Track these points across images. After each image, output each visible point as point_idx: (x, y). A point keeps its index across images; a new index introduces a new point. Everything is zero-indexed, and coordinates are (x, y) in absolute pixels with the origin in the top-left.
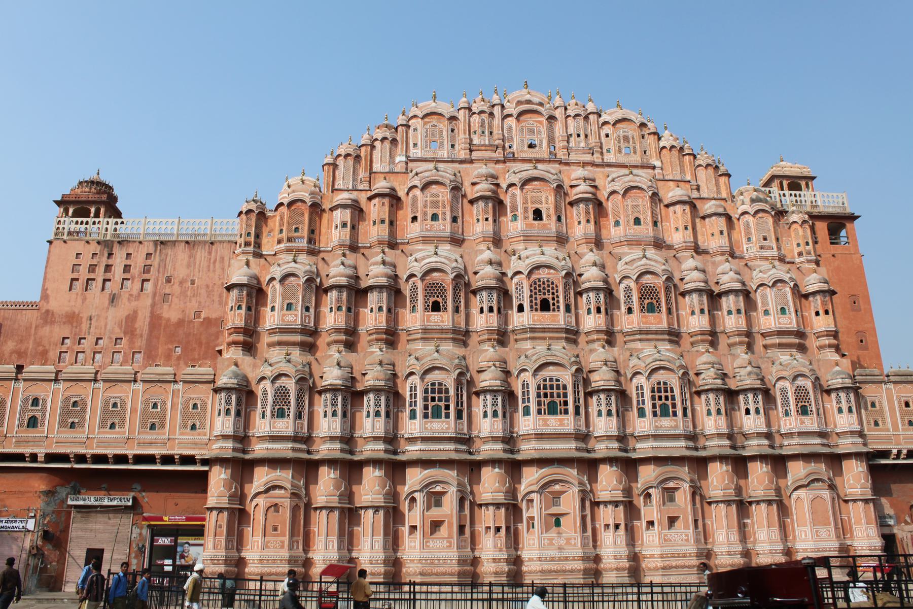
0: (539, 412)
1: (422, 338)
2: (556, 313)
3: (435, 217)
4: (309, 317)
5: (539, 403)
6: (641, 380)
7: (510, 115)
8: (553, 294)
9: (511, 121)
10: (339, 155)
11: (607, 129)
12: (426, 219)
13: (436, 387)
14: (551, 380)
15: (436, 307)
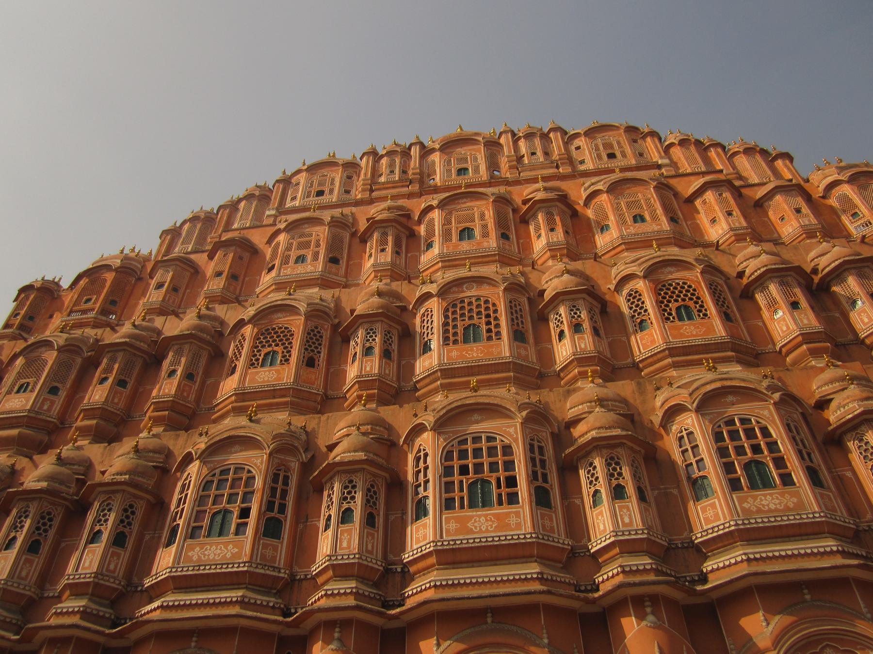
0: (448, 504)
1: (234, 409)
2: (494, 342)
3: (301, 259)
4: (53, 403)
5: (449, 487)
6: (689, 421)
7: (433, 150)
8: (488, 316)
9: (436, 157)
10: (184, 222)
11: (577, 142)
12: (287, 263)
13: (230, 477)
14: (477, 439)
15: (269, 359)
